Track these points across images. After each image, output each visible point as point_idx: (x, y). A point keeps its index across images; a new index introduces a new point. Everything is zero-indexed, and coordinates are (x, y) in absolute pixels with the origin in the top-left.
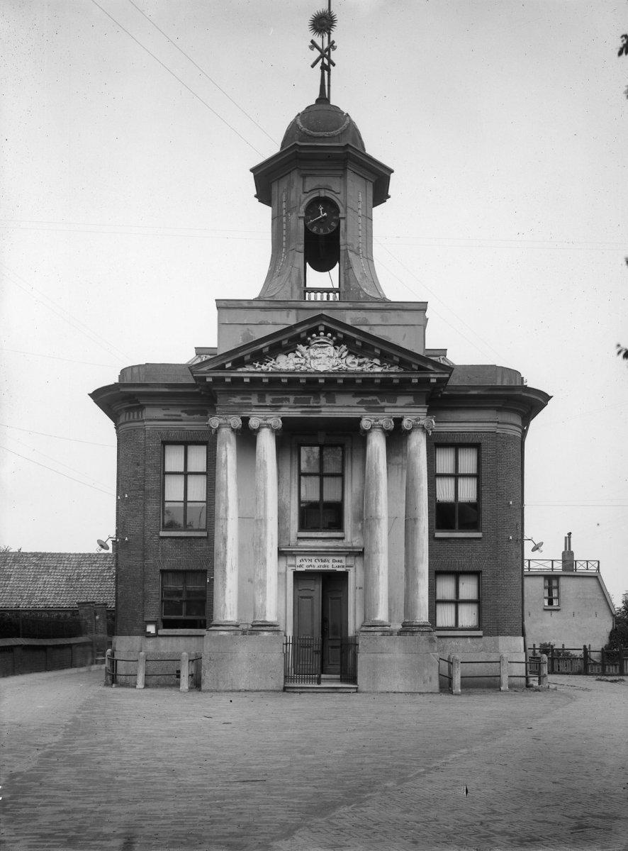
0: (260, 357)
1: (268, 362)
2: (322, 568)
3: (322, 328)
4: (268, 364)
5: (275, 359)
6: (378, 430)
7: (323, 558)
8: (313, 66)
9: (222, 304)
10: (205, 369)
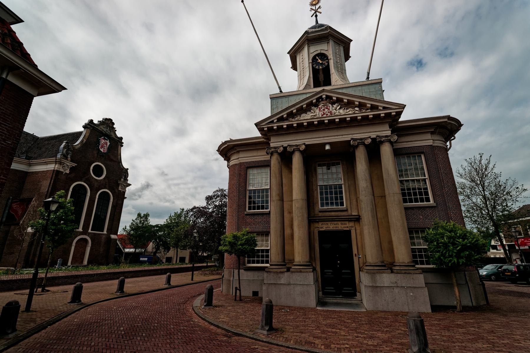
0: (291, 115)
1: (296, 117)
2: (335, 229)
3: (324, 96)
4: (296, 119)
5: (300, 116)
7: (335, 222)
9: (272, 96)
10: (263, 124)
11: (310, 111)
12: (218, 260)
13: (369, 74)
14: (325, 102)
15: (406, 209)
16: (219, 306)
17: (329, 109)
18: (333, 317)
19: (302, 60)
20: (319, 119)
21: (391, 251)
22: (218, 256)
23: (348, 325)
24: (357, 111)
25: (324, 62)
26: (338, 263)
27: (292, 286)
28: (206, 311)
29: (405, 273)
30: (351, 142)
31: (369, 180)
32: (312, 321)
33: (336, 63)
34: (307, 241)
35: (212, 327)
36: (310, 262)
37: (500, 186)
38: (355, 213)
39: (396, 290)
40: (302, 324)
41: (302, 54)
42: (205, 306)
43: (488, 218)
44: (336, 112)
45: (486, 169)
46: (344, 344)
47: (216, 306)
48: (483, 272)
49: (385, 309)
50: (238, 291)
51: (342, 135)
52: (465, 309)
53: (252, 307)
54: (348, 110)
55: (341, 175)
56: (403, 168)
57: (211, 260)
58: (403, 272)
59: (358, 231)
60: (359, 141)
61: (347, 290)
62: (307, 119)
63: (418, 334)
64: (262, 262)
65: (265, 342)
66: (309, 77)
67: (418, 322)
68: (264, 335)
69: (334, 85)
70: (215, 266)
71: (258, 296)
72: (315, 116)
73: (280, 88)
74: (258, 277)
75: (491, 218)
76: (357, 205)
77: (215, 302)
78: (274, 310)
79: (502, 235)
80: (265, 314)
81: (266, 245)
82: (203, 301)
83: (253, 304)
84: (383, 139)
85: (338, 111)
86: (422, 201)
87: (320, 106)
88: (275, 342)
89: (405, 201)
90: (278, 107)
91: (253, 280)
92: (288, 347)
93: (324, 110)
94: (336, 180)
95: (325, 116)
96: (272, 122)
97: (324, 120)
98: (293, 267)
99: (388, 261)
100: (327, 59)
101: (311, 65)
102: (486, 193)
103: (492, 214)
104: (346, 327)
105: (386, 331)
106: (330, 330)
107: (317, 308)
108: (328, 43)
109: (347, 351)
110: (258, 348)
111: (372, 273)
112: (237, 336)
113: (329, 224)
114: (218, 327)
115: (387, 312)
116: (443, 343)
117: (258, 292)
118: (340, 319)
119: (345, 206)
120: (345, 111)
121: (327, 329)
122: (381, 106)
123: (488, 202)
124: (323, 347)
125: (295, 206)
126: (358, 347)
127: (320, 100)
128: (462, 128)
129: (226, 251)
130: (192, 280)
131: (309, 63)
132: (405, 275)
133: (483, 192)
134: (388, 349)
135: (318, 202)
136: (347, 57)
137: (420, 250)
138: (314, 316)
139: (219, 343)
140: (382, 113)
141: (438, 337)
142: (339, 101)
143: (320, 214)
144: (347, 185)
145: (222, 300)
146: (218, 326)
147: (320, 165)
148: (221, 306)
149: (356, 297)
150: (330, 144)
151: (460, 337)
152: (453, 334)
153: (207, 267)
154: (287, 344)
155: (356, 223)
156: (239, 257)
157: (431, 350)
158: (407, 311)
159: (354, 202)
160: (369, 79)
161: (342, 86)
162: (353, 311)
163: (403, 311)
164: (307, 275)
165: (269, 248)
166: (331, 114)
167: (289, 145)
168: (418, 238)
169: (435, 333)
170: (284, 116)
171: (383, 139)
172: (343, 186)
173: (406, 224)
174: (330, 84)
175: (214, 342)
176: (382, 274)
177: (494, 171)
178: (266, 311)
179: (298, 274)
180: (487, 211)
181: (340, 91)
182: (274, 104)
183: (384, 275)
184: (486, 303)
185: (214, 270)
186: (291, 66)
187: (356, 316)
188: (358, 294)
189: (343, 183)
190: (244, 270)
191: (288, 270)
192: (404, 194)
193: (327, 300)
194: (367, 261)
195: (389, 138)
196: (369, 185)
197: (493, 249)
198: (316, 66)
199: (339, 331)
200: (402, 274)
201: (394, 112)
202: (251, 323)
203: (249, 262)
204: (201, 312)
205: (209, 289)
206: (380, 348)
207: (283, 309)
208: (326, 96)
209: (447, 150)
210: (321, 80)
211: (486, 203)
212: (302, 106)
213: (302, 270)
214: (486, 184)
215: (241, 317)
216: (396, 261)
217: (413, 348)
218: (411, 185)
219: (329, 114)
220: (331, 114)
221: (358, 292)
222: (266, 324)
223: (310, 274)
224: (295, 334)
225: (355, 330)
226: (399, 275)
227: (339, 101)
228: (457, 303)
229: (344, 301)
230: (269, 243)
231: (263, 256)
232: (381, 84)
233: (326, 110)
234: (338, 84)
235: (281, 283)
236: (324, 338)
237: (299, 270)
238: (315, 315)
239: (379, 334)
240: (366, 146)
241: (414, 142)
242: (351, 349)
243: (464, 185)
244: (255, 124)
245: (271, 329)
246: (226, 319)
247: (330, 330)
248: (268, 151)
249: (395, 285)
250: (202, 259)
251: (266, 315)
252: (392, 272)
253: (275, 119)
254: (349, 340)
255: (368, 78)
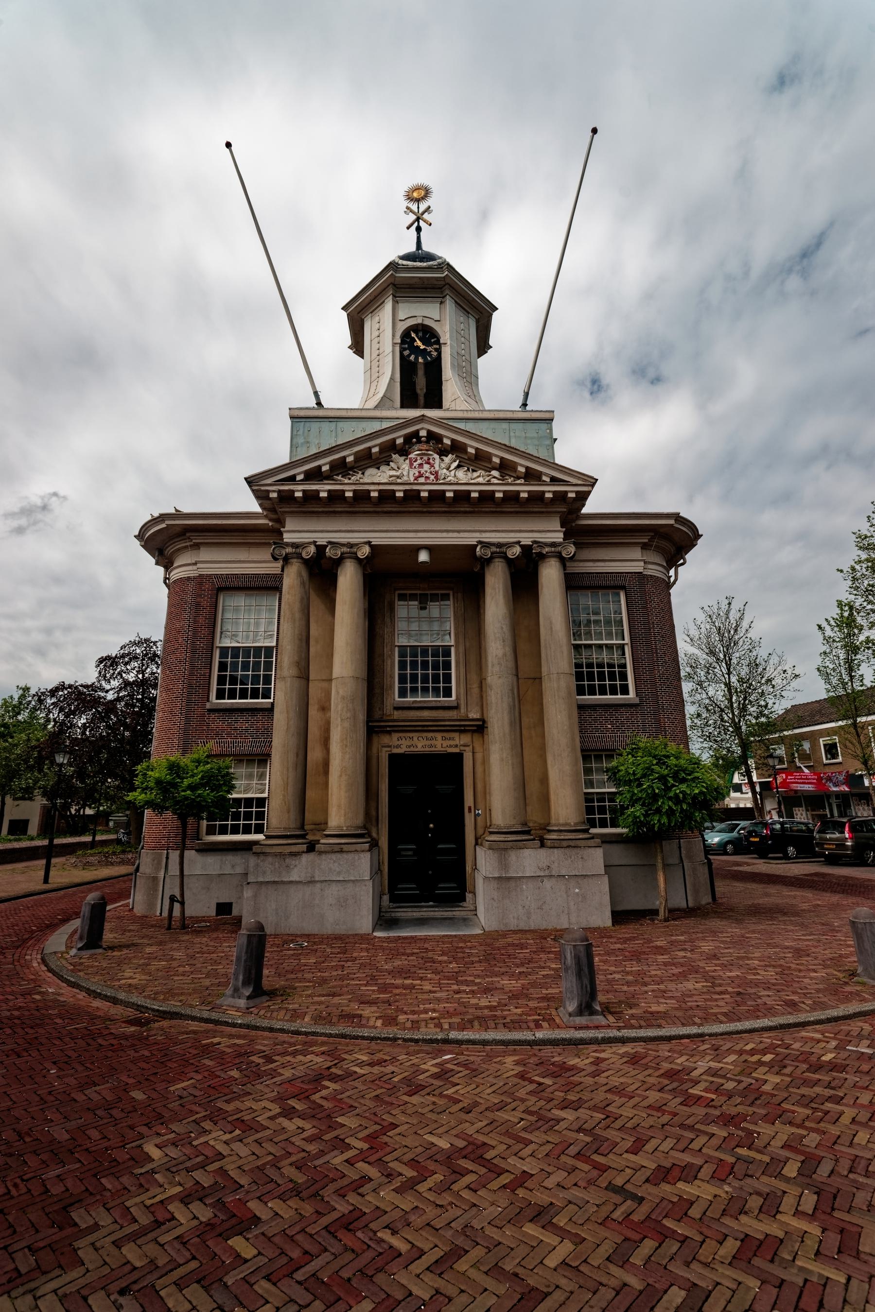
0: (341, 468)
1: (353, 475)
2: (427, 749)
3: (423, 433)
5: (363, 474)
6: (500, 560)
7: (430, 735)
8: (408, 228)
9: (296, 413)
10: (269, 481)
11: (389, 465)
12: (127, 825)
13: (526, 395)
14: (425, 447)
15: (581, 707)
16: (120, 947)
17: (432, 466)
18: (408, 951)
19: (377, 333)
20: (407, 487)
21: (545, 799)
22: (127, 816)
23: (440, 969)
24: (494, 477)
25: (429, 349)
26: (431, 829)
27: (318, 885)
28: (81, 964)
29: (568, 847)
30: (478, 549)
31: (509, 642)
32: (361, 964)
33: (457, 356)
34: (361, 779)
35: (97, 1003)
36: (364, 827)
37: (757, 665)
38: (474, 714)
39: (548, 884)
40: (335, 973)
41: (377, 319)
42: (79, 949)
43: (730, 729)
44: (448, 474)
45: (736, 630)
46: (426, 1011)
47: (112, 948)
48: (714, 838)
49: (523, 926)
50: (177, 906)
51: (459, 531)
52: (675, 914)
53: (212, 944)
54: (475, 474)
55: (450, 626)
56: (583, 617)
57: (107, 825)
58: (565, 844)
59: (479, 756)
60: (494, 549)
61: (446, 887)
62: (379, 484)
63: (579, 974)
64: (247, 830)
65: (241, 1026)
66: (392, 379)
67: (582, 949)
68: (238, 1009)
69: (448, 410)
70: (118, 841)
71: (230, 913)
72: (398, 477)
73: (316, 394)
74: (233, 866)
75: (738, 728)
76: (482, 697)
77: (111, 936)
78: (268, 945)
79: (751, 762)
80: (243, 959)
81: (260, 787)
82: (77, 936)
83: (215, 935)
84: (547, 549)
85: (453, 472)
86: (614, 692)
87: (412, 456)
88: (266, 1023)
89: (580, 691)
90: (308, 442)
91: (220, 875)
92: (297, 1033)
93: (421, 465)
94: (438, 634)
95: (422, 480)
96: (292, 479)
97: (419, 491)
98: (322, 841)
99: (535, 822)
100: (438, 342)
101: (398, 349)
102: (734, 679)
103: (740, 721)
104: (436, 972)
105: (520, 973)
106: (399, 982)
107: (375, 934)
108: (441, 303)
109: (432, 1026)
110: (219, 1043)
111: (501, 850)
112: (165, 1019)
113: (415, 739)
114: (115, 1001)
115: (525, 932)
116: (625, 988)
117: (230, 904)
118: (424, 955)
119: (454, 697)
120: (469, 474)
121: (393, 981)
122: (547, 475)
123: (734, 698)
124: (379, 1023)
125: (338, 693)
126: (457, 1014)
127: (414, 440)
128: (699, 542)
129: (149, 804)
130: (46, 880)
131: (394, 344)
132: (567, 851)
133: (726, 676)
134: (519, 1011)
135: (392, 687)
136: (483, 347)
137: (601, 797)
138: (366, 954)
139: (115, 1042)
140: (549, 491)
141: (617, 976)
142: (457, 448)
143: (397, 714)
144: (461, 649)
145: (130, 931)
146: (114, 998)
147: (402, 597)
148: (127, 946)
149: (464, 904)
150: (429, 548)
151: (658, 972)
152: (645, 968)
153: (93, 844)
154: (293, 1026)
155: (476, 736)
156: (183, 818)
157: (601, 1004)
158: (566, 926)
159: (475, 690)
160: (528, 408)
161: (466, 415)
162: (455, 936)
163: (558, 928)
164: (356, 858)
165: (265, 795)
166: (437, 478)
167: (330, 543)
168: (600, 770)
169: (613, 969)
170: (324, 468)
171: (547, 549)
172: (453, 650)
173: (578, 739)
174: (438, 405)
175: (100, 1041)
176: (521, 851)
177: (749, 635)
178: (246, 952)
179: (334, 856)
180: (731, 716)
181: (461, 425)
182: (301, 432)
183: (527, 852)
184: (710, 900)
185: (114, 853)
186: (350, 343)
187: (461, 945)
188: (469, 896)
189: (452, 643)
190: (197, 851)
191: (311, 848)
192: (579, 676)
193: (398, 914)
194: (494, 822)
195: (559, 549)
196: (509, 650)
197: (735, 791)
198: (409, 356)
199: (418, 982)
200: (562, 850)
201: (572, 492)
202: (207, 982)
203: (211, 831)
204: (67, 965)
205: (94, 906)
206: (502, 1010)
207: (292, 941)
208: (429, 432)
209: (669, 586)
210: (418, 391)
211: (731, 698)
212: (370, 448)
213: (345, 848)
214: (734, 661)
215: (181, 969)
216: (553, 821)
217: (567, 1003)
218: (595, 657)
219: (432, 477)
220: (437, 478)
221: (470, 892)
222: (246, 983)
223: (362, 855)
224: (316, 999)
225: (455, 977)
226: (555, 850)
227: (457, 448)
228: (661, 903)
229: (439, 913)
230: (267, 782)
231: (248, 815)
232: (551, 424)
233: (426, 467)
234: (458, 408)
235: (291, 879)
236: (384, 1002)
237: (336, 848)
238: (367, 950)
239: (505, 982)
240: (510, 562)
241: (607, 564)
242: (442, 1021)
243: (696, 661)
244: (246, 479)
245: (259, 992)
246: (139, 978)
247: (399, 982)
248: (277, 552)
249: (547, 873)
250: (80, 825)
251: (246, 961)
252: (542, 845)
253: (299, 472)
254: (439, 1000)
255: (525, 405)
